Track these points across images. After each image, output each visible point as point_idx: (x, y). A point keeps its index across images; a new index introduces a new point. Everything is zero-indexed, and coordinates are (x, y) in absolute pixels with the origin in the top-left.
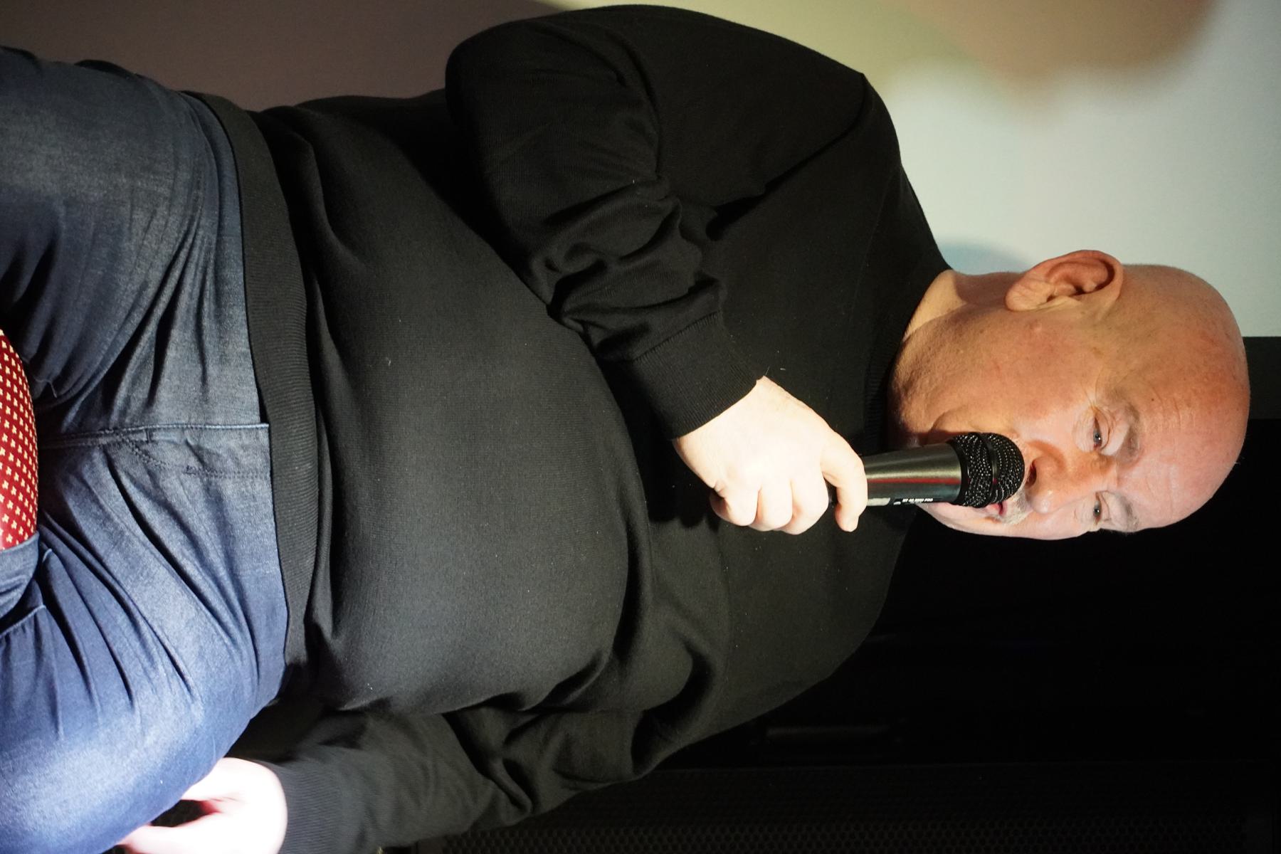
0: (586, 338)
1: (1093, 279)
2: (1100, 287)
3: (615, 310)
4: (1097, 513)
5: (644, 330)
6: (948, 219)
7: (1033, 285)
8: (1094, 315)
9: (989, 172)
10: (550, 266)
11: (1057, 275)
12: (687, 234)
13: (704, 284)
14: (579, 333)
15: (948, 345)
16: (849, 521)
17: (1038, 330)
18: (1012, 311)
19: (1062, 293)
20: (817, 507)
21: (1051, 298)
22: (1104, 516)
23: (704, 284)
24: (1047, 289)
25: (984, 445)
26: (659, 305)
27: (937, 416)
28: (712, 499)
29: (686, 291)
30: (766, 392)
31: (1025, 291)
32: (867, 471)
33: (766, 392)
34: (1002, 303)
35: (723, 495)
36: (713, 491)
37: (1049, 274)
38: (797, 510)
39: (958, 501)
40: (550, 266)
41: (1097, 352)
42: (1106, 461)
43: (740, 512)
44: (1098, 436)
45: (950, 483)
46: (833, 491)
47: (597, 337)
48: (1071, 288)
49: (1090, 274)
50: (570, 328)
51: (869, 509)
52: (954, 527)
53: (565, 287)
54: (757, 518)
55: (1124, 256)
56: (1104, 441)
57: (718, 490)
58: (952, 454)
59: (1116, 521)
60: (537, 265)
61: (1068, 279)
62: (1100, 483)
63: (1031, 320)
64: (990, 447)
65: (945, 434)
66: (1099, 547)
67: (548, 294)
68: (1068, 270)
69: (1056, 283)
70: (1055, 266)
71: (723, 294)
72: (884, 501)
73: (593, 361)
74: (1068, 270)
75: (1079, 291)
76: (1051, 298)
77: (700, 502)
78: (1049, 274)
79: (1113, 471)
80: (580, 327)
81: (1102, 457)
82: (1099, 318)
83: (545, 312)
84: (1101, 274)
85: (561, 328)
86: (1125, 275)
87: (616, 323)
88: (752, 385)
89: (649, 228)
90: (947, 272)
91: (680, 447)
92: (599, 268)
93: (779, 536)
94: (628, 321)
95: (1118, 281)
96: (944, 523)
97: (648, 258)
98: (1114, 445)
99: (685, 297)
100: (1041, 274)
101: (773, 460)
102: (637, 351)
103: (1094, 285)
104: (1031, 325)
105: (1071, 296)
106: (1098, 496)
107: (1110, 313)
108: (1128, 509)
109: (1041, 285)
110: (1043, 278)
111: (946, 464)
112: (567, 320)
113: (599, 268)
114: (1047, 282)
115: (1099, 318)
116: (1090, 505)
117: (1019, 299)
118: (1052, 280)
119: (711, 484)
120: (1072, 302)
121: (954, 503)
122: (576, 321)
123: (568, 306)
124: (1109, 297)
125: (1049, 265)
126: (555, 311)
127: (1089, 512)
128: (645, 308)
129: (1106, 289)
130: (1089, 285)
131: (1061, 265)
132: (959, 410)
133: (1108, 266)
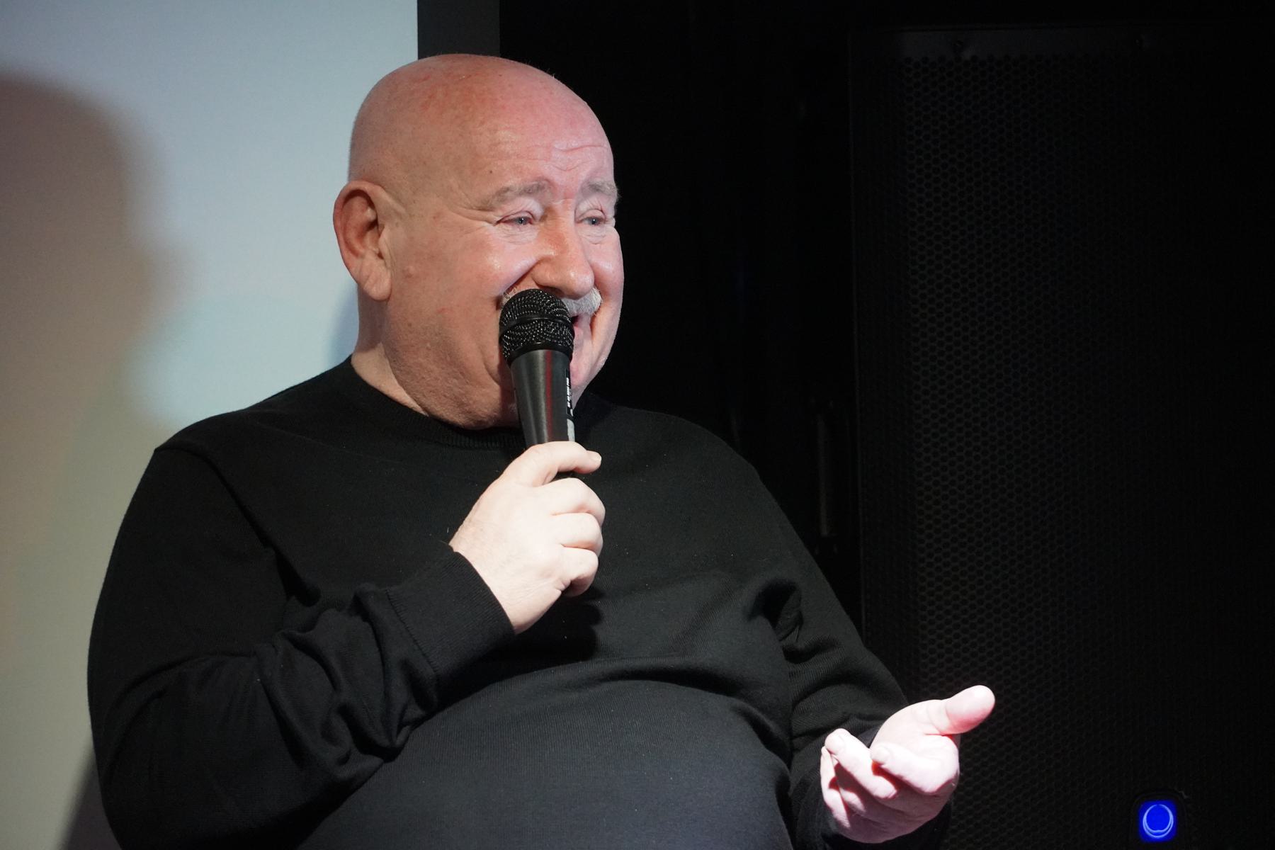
0: (417, 723)
1: (363, 211)
2: (371, 204)
3: (387, 695)
4: (595, 221)
5: (406, 665)
6: (306, 361)
7: (365, 273)
8: (398, 214)
9: (250, 315)
10: (344, 760)
11: (357, 246)
12: (310, 625)
13: (359, 607)
14: (412, 730)
15: (421, 360)
16: (592, 460)
17: (412, 269)
18: (389, 298)
19: (376, 243)
20: (577, 490)
21: (380, 256)
22: (599, 214)
23: (359, 607)
24: (370, 258)
25: (512, 328)
26: (380, 650)
27: (488, 377)
28: (571, 595)
29: (367, 624)
30: (465, 542)
31: (371, 281)
32: (540, 442)
33: (465, 542)
34: (382, 303)
35: (568, 582)
36: (563, 592)
38: (580, 509)
39: (568, 353)
40: (344, 760)
42: (548, 213)
43: (585, 565)
44: (522, 221)
45: (549, 360)
46: (562, 475)
47: (415, 712)
48: (369, 233)
49: (358, 214)
50: (407, 739)
51: (579, 440)
52: (604, 359)
53: (366, 745)
54: (590, 547)
56: (526, 215)
57: (563, 587)
58: (522, 360)
59: (607, 203)
60: (345, 773)
61: (361, 236)
62: (567, 220)
63: (403, 277)
64: (514, 323)
65: (501, 367)
66: (630, 221)
67: (375, 761)
69: (364, 247)
70: (349, 249)
71: (369, 587)
72: (570, 424)
73: (440, 715)
74: (352, 235)
75: (374, 225)
76: (380, 256)
77: (576, 604)
79: (558, 204)
80: (406, 730)
81: (543, 218)
82: (401, 209)
83: (389, 765)
84: (357, 203)
85: (407, 747)
87: (400, 694)
88: (458, 556)
89: (304, 663)
90: (355, 363)
91: (521, 626)
92: (346, 712)
93: (607, 527)
94: (398, 681)
95: (367, 187)
96: (598, 368)
97: (334, 662)
98: (532, 205)
99: (371, 624)
100: (356, 262)
101: (532, 534)
102: (427, 672)
103: (369, 210)
106: (578, 221)
108: (596, 189)
109: (367, 264)
111: (532, 365)
112: (399, 740)
113: (346, 712)
114: (363, 257)
115: (401, 209)
116: (588, 229)
117: (380, 287)
118: (362, 251)
119: (558, 593)
120: (386, 235)
121: (571, 358)
122: (399, 732)
123: (383, 741)
124: (382, 197)
125: (348, 254)
126: (389, 754)
127: (595, 230)
128: (383, 664)
130: (369, 214)
132: (482, 353)
133: (349, 196)
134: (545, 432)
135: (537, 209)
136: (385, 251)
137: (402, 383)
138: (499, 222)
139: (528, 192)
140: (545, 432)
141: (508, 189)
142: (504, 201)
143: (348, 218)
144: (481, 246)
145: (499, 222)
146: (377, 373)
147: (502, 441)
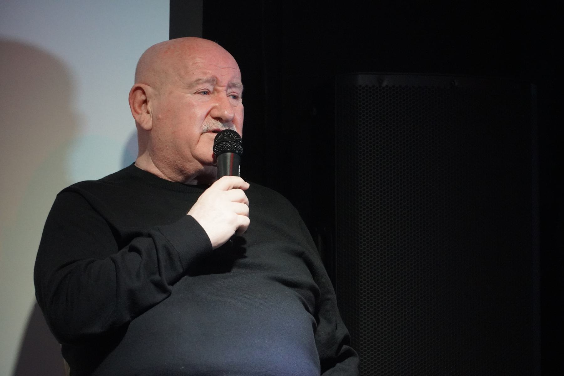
2: (144, 93)
7: (142, 119)
8: (155, 95)
11: (138, 110)
21: (148, 112)
24: (145, 114)
37: (138, 113)
41: (171, 93)
48: (143, 105)
55: (131, 84)
61: (140, 106)
68: (136, 106)
70: (135, 111)
74: (136, 106)
75: (145, 102)
76: (148, 112)
78: (138, 113)
82: (157, 93)
84: (139, 92)
86: (140, 83)
95: (142, 86)
100: (138, 117)
104: (158, 119)
105: (147, 104)
107: (154, 88)
109: (143, 116)
110: (139, 116)
115: (157, 93)
118: (140, 112)
120: (149, 104)
125: (134, 113)
129: (145, 91)
130: (143, 98)
131: (134, 108)
134: (229, 169)
135: (211, 88)
136: (150, 109)
137: (157, 166)
138: (195, 93)
139: (207, 81)
140: (229, 169)
141: (200, 79)
142: (198, 84)
143: (134, 99)
144: (190, 106)
145: (195, 93)
146: (147, 165)
147: (204, 181)
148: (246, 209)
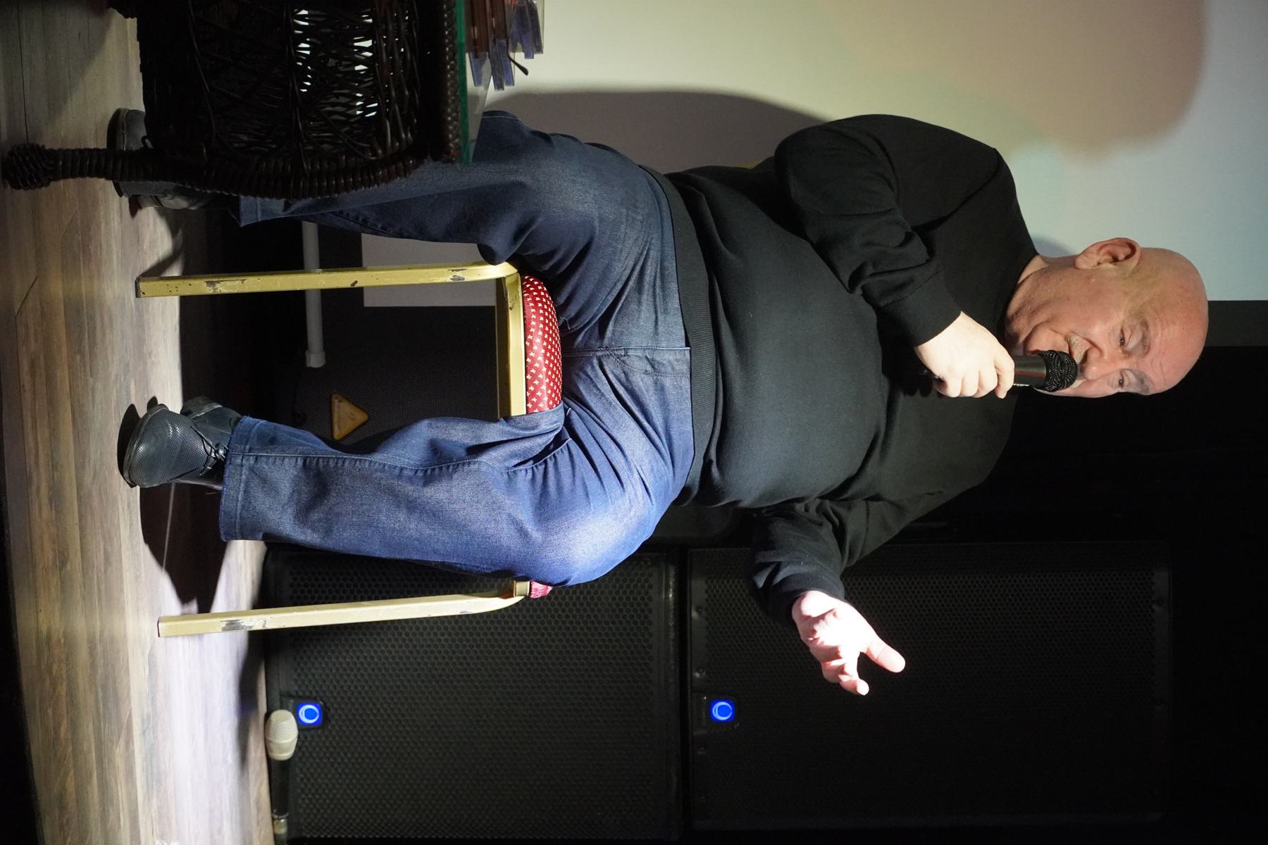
2: (1127, 257)
4: (1121, 384)
19: (1106, 261)
22: (1126, 383)
37: (1101, 248)
41: (1126, 294)
49: (1122, 251)
59: (1132, 387)
61: (1109, 253)
63: (1089, 275)
66: (1122, 401)
70: (1103, 245)
75: (1115, 260)
84: (1128, 250)
88: (958, 315)
95: (1137, 255)
100: (1095, 249)
101: (966, 358)
107: (1133, 272)
120: (1111, 266)
124: (1133, 263)
130: (1121, 257)
133: (1132, 247)
148: (970, 392)
